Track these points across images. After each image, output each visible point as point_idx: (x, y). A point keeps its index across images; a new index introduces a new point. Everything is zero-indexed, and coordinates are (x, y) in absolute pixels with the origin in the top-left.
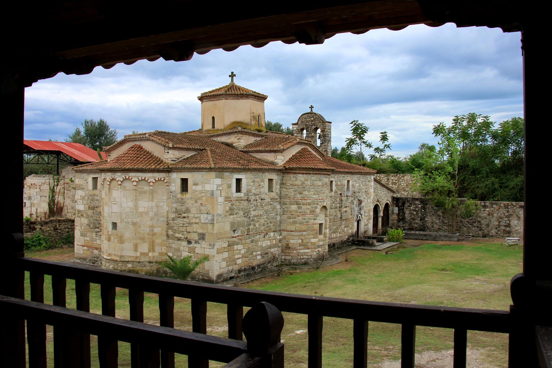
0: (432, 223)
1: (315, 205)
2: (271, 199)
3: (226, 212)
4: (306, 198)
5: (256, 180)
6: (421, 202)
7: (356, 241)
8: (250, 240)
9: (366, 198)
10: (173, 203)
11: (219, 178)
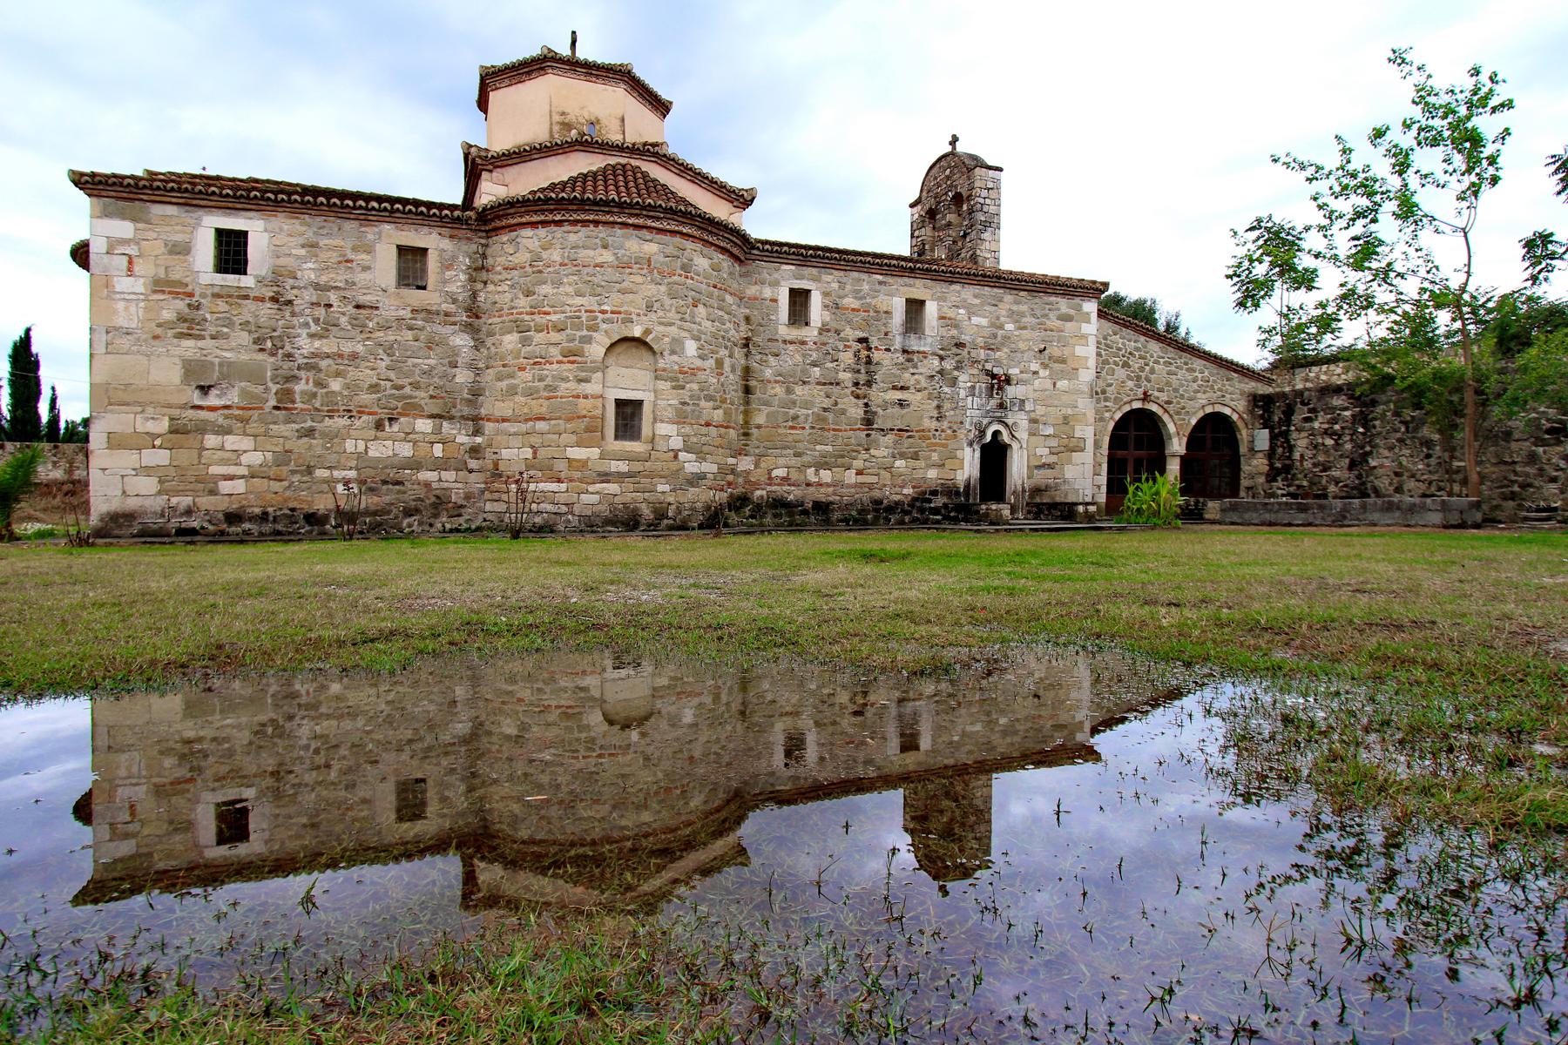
0: (1397, 474)
3: (159, 325)
4: (547, 309)
5: (323, 242)
6: (1351, 397)
8: (297, 426)
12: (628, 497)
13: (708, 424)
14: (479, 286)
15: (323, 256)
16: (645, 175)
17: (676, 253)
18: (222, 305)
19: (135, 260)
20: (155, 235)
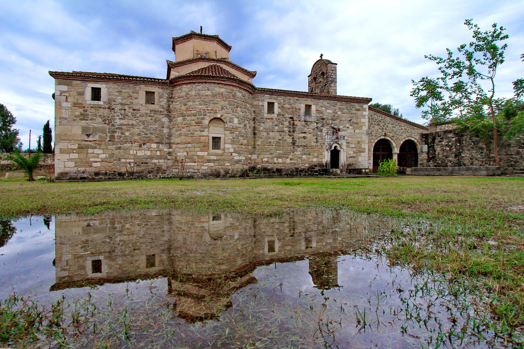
0: (471, 159)
4: (191, 109)
5: (123, 91)
6: (455, 134)
8: (116, 146)
12: (216, 167)
13: (242, 144)
14: (171, 103)
15: (123, 95)
16: (221, 68)
17: (231, 91)
18: (93, 110)
19: (68, 97)
20: (74, 90)
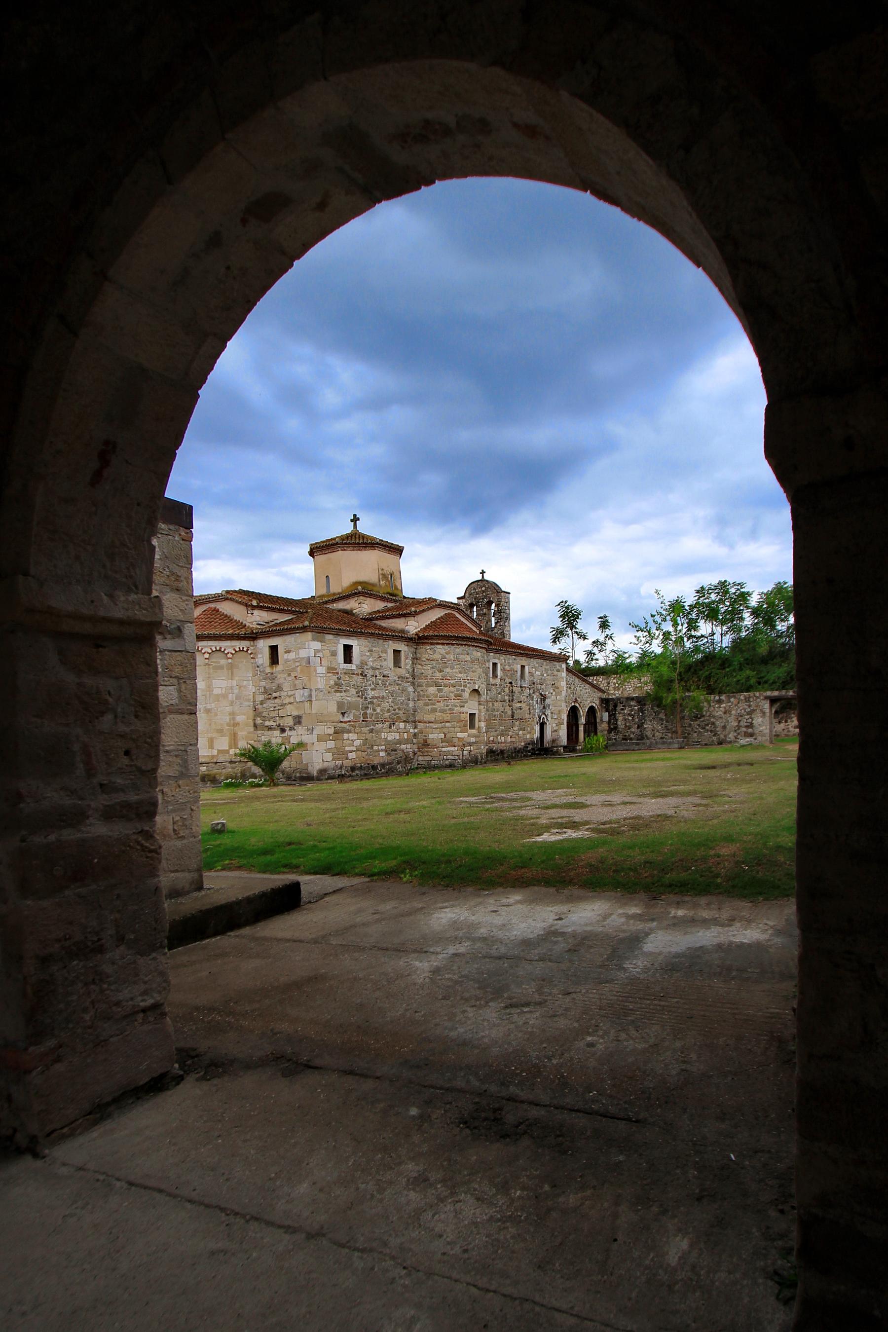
1: (461, 687)
2: (398, 677)
3: (330, 687)
4: (448, 678)
7: (537, 750)
9: (554, 693)
10: (261, 680)
11: (318, 641)
14: (415, 666)
